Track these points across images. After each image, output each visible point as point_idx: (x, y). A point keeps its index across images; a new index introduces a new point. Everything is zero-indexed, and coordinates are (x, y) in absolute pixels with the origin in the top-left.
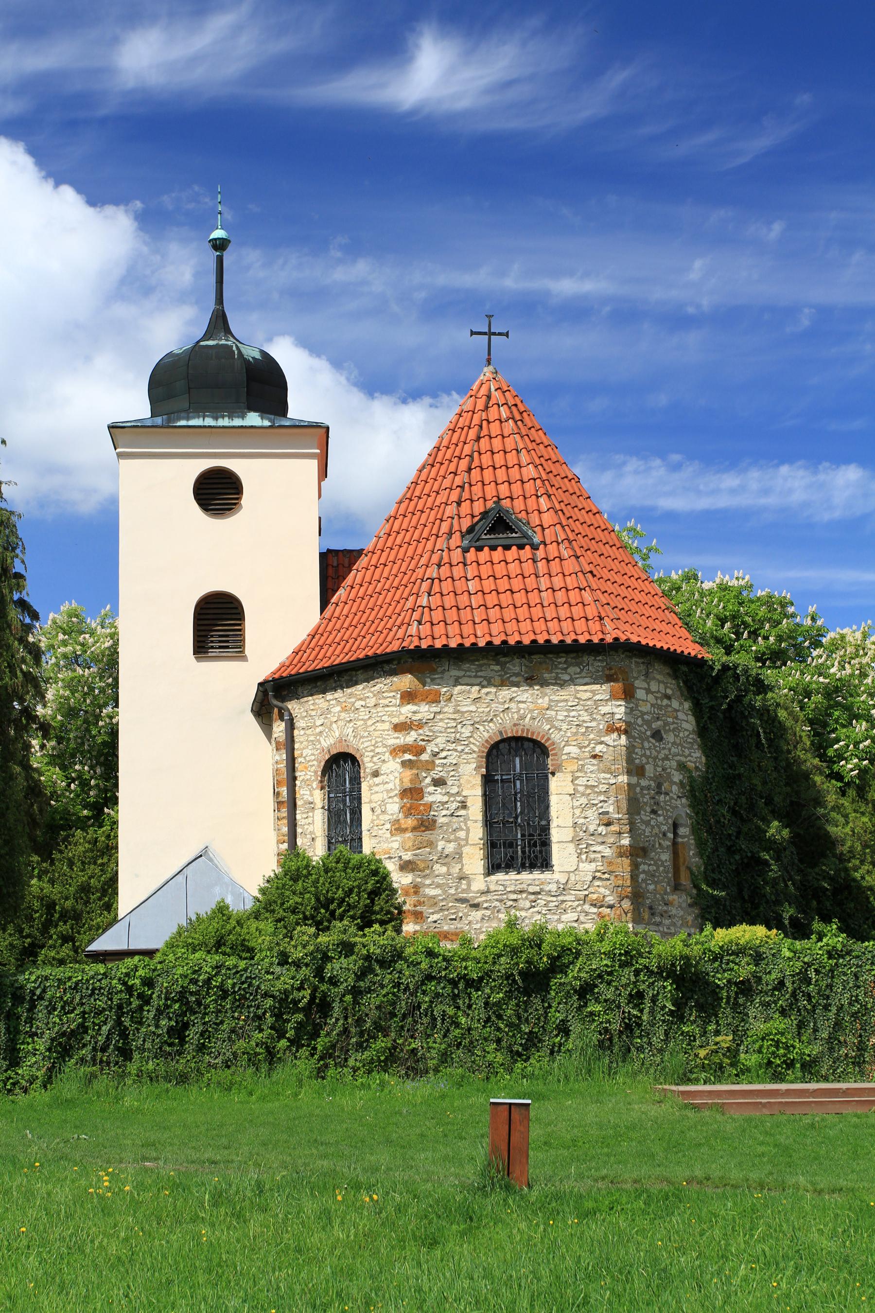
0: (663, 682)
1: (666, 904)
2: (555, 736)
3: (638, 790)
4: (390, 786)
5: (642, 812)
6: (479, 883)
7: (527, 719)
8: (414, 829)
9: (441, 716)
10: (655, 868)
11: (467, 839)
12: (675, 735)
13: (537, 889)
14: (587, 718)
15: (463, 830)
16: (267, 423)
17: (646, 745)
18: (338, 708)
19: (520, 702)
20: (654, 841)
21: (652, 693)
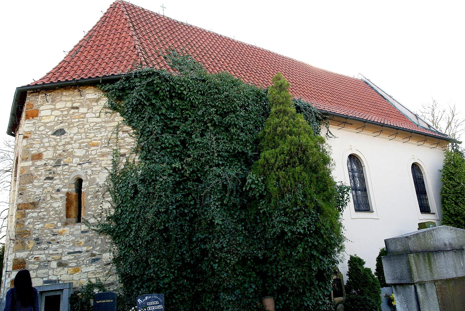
0: (71, 101)
1: (53, 235)
3: (32, 169)
5: (35, 181)
10: (45, 213)
21: (58, 110)
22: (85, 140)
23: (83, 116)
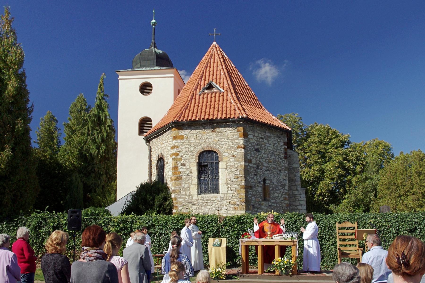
0: (260, 133)
1: (259, 205)
2: (221, 150)
3: (249, 167)
4: (170, 167)
5: (250, 175)
6: (195, 197)
7: (212, 144)
8: (175, 180)
9: (184, 144)
10: (255, 193)
11: (192, 183)
12: (265, 151)
13: (214, 199)
14: (231, 144)
15: (190, 180)
16: (159, 68)
17: (252, 153)
18: (160, 144)
19: (209, 139)
20: (255, 184)
21: (256, 136)
22: (268, 158)
23: (265, 144)
